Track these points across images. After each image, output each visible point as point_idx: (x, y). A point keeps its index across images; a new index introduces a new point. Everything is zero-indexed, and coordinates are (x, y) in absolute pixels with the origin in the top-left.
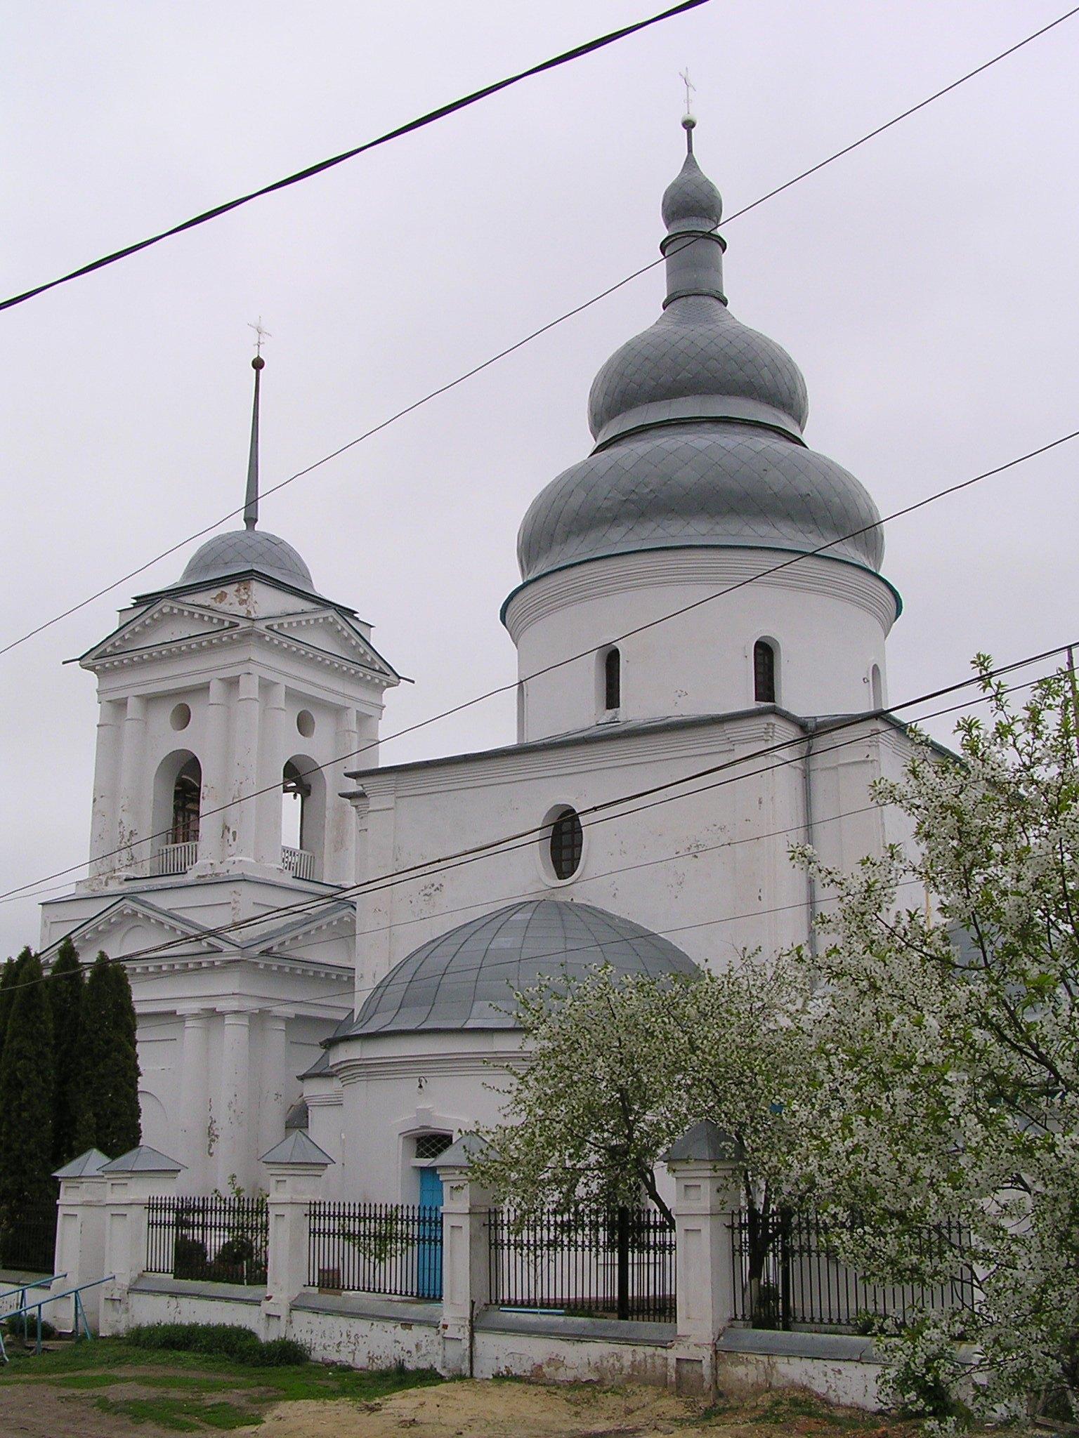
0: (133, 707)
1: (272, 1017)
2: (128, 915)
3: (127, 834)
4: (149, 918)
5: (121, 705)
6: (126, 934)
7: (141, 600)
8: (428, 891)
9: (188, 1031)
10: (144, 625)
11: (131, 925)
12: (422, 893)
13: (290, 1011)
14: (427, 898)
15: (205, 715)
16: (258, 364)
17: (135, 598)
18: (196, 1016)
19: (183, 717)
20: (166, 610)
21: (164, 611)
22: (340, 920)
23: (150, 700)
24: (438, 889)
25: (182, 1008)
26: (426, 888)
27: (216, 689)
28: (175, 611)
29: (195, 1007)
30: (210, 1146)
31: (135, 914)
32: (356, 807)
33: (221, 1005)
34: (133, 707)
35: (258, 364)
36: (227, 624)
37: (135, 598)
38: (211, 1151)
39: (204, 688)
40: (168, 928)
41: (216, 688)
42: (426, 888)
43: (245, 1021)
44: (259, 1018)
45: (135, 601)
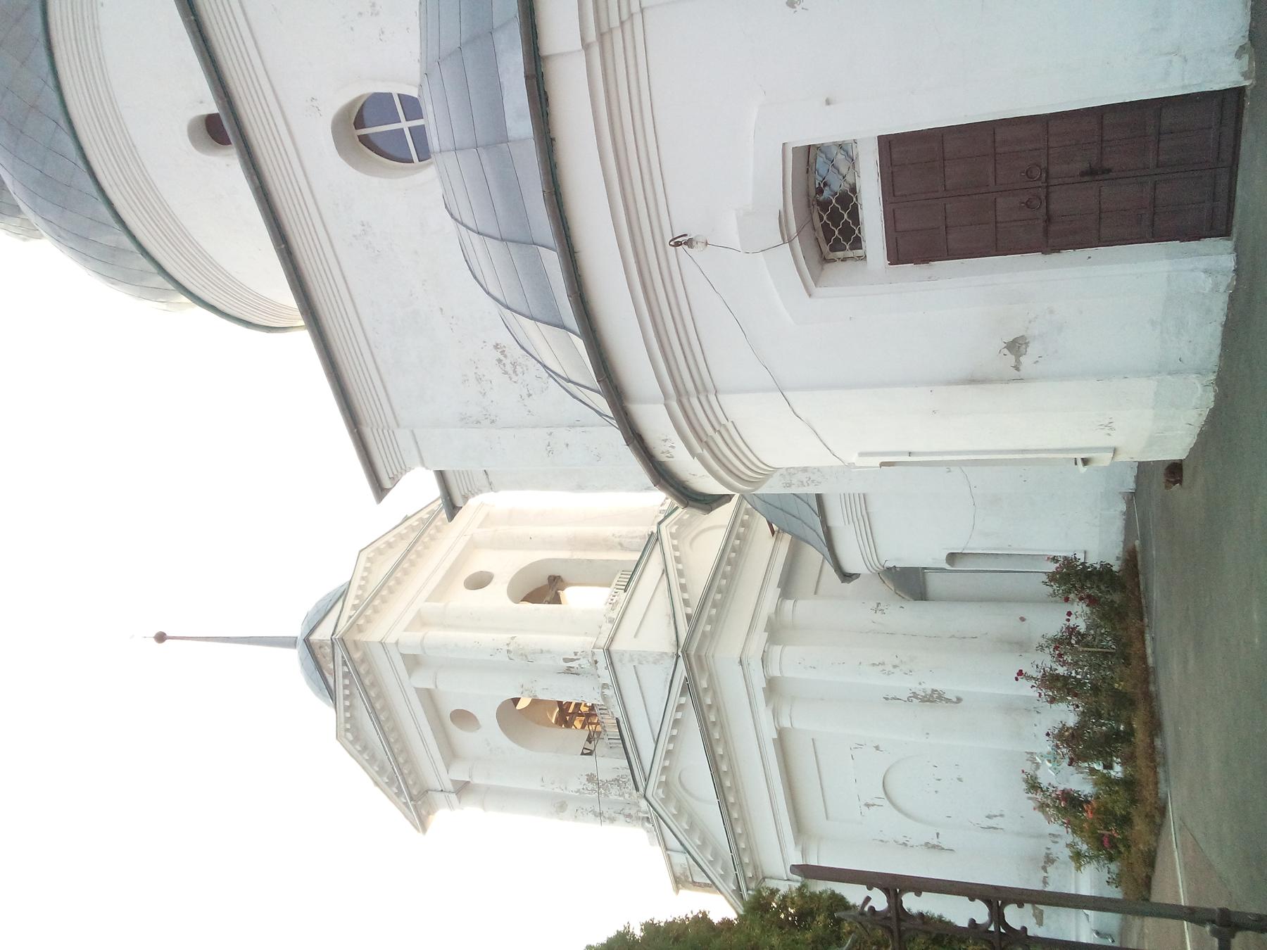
0: (460, 774)
1: (776, 617)
3: (590, 786)
4: (664, 768)
5: (462, 789)
6: (691, 794)
8: (509, 368)
9: (796, 725)
11: (678, 785)
12: (515, 378)
13: (773, 592)
14: (519, 369)
15: (455, 694)
16: (161, 638)
18: (776, 714)
19: (463, 717)
22: (673, 536)
23: (451, 753)
24: (503, 352)
25: (770, 733)
26: (506, 373)
27: (422, 680)
28: (348, 726)
30: (948, 700)
32: (466, 498)
33: (759, 683)
38: (955, 700)
41: (422, 680)
42: (506, 373)
43: (777, 649)
44: (776, 632)
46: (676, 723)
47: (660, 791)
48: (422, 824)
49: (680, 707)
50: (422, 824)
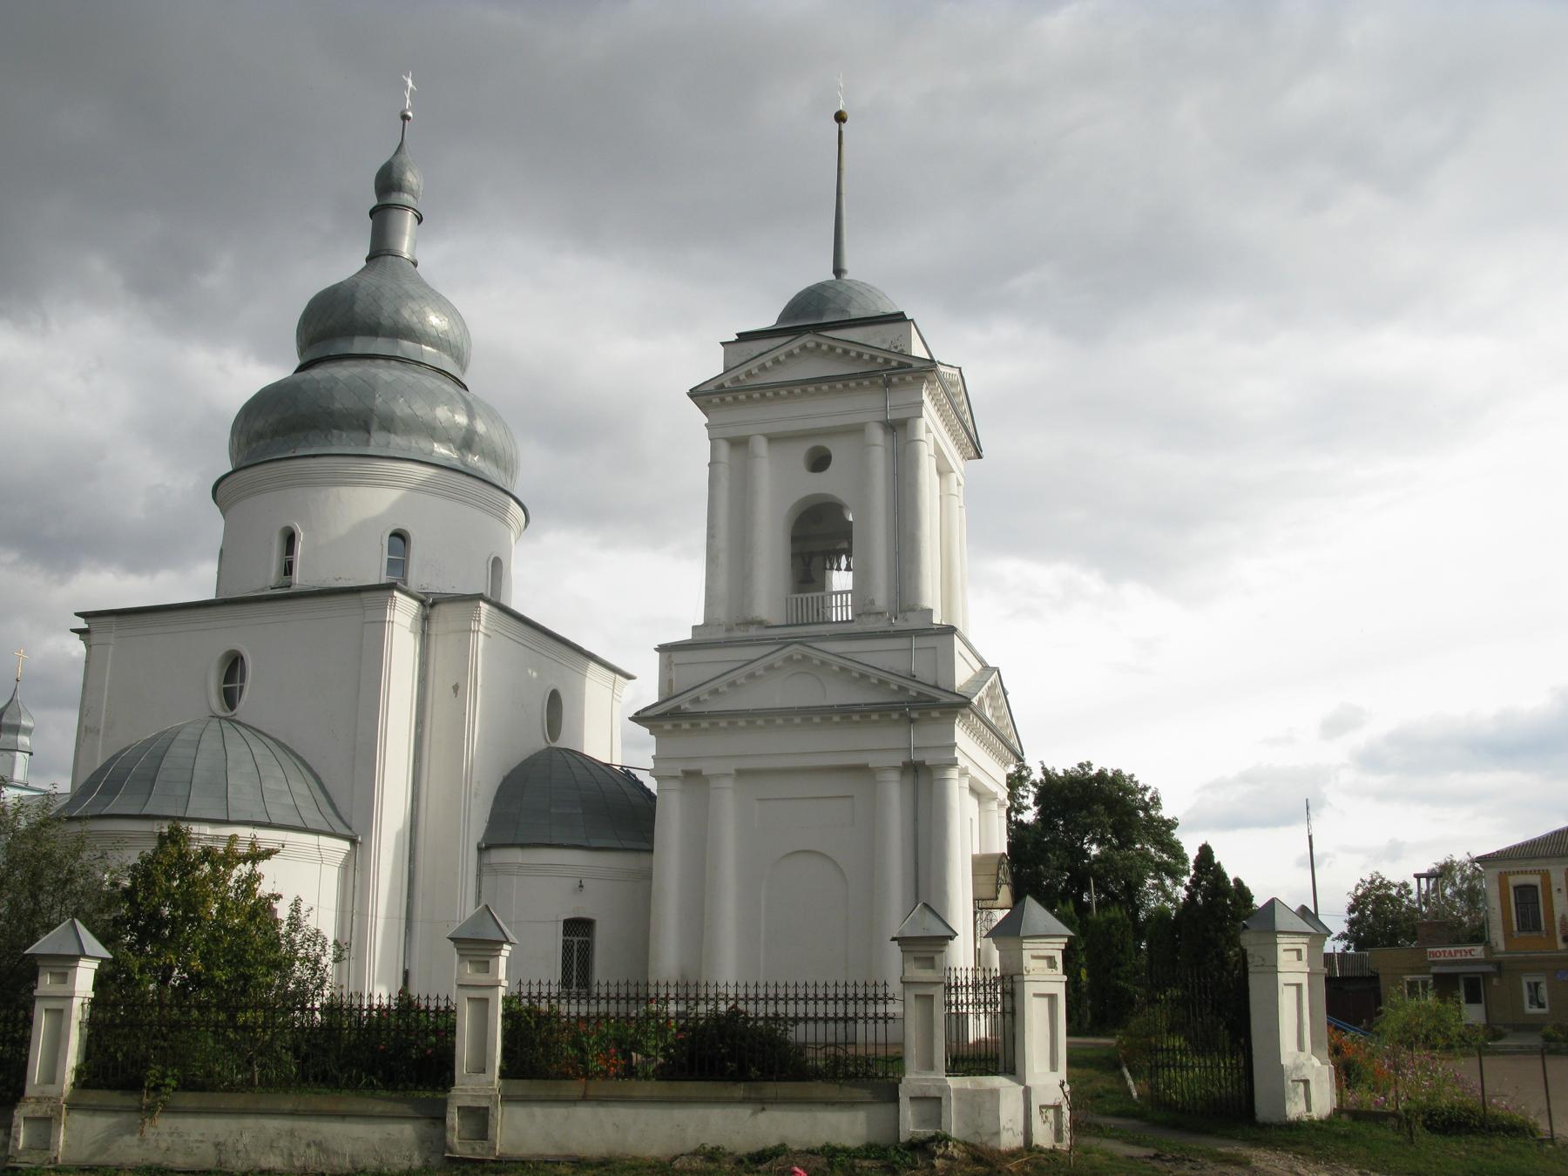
0: (761, 446)
2: (798, 661)
5: (739, 444)
7: (744, 337)
10: (776, 361)
17: (737, 334)
19: (819, 462)
20: (811, 345)
21: (809, 345)
25: (872, 761)
28: (824, 348)
29: (899, 759)
31: (805, 658)
34: (761, 446)
35: (840, 118)
36: (894, 364)
37: (737, 334)
39: (858, 430)
40: (857, 675)
45: (737, 338)
46: (881, 682)
47: (800, 657)
48: (694, 394)
49: (902, 689)
50: (694, 394)
